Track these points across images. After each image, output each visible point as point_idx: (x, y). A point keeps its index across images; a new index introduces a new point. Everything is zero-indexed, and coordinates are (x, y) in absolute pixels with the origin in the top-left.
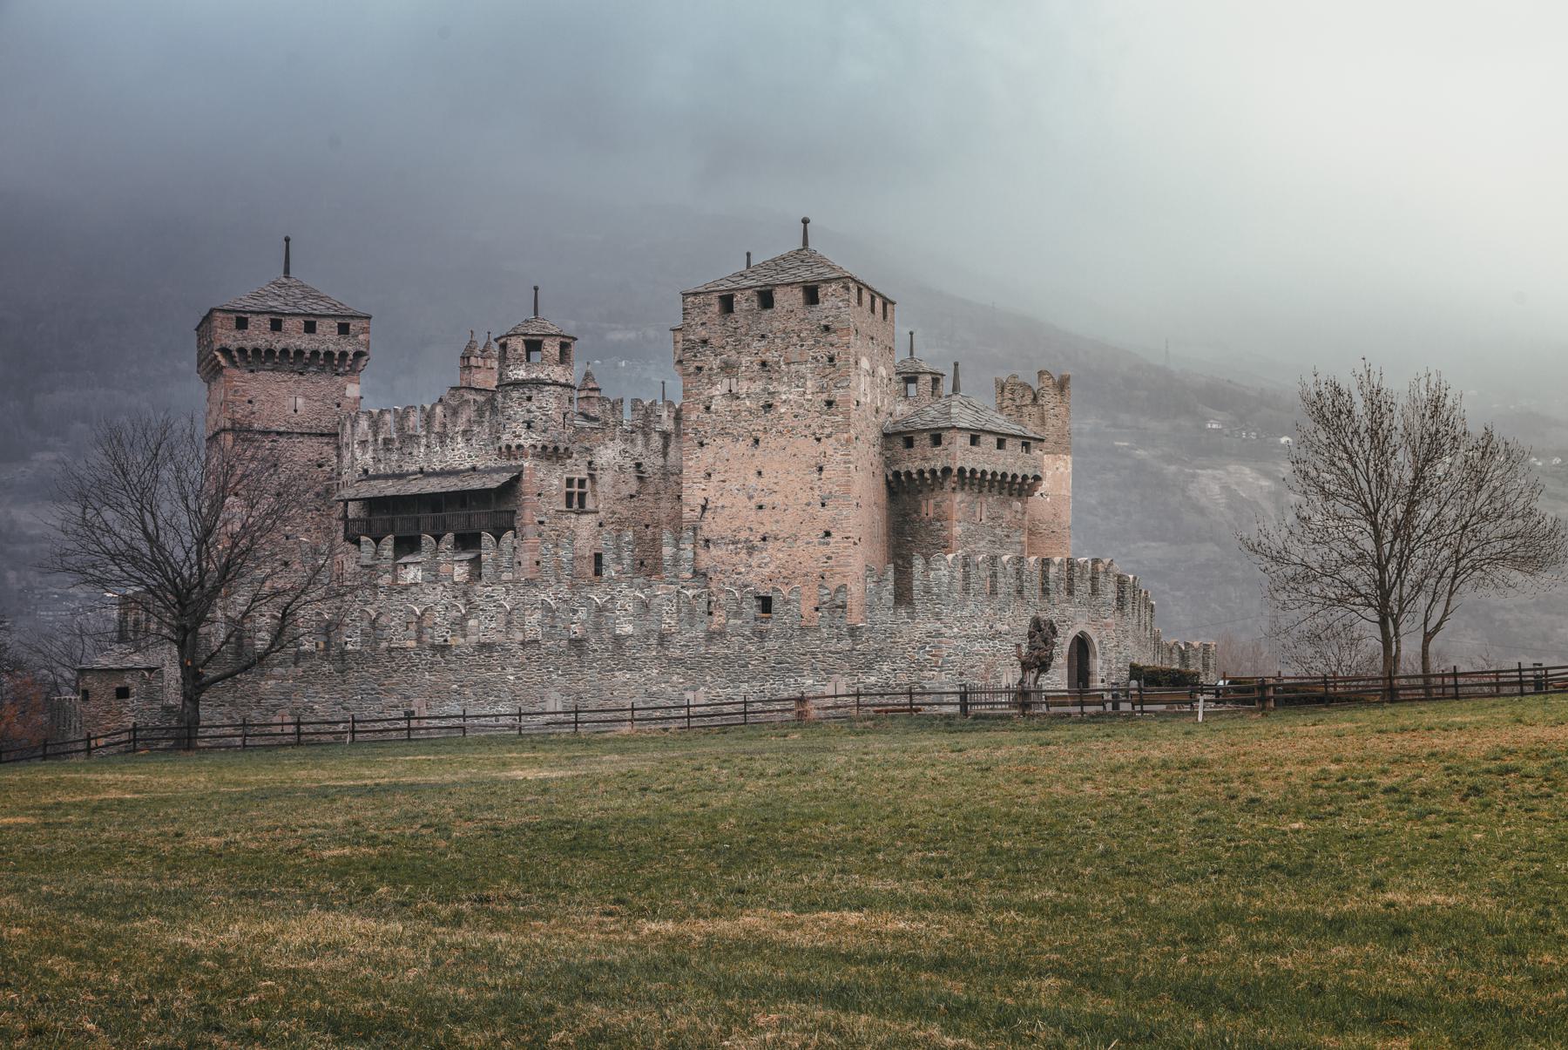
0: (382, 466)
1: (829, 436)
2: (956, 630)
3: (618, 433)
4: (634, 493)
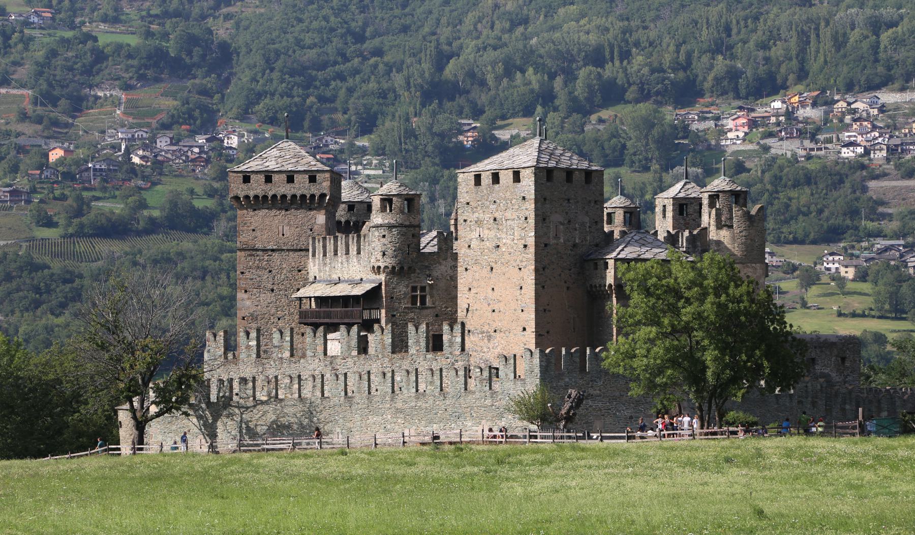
0: (322, 274)
1: (525, 268)
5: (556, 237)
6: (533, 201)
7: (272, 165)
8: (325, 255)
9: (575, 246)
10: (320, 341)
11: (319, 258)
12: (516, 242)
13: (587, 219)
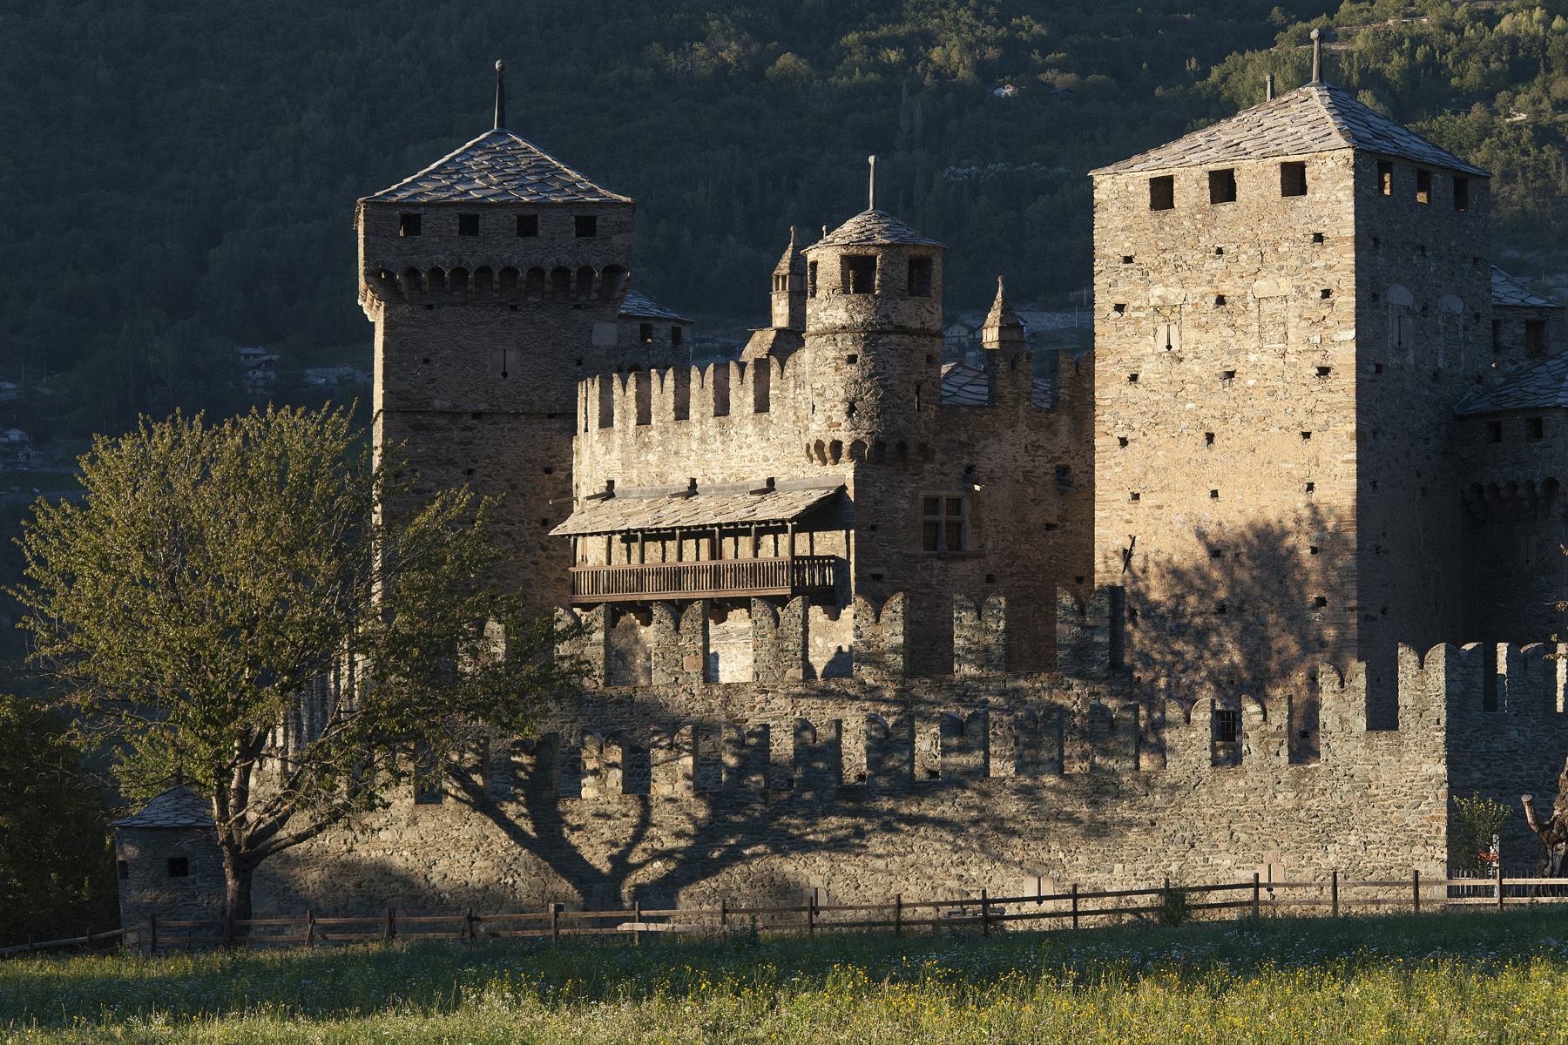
0: (634, 473)
2: (1477, 775)
3: (1022, 413)
4: (1052, 520)
5: (1400, 349)
6: (1350, 245)
7: (477, 189)
9: (1436, 376)
10: (690, 643)
11: (624, 432)
12: (1292, 359)
13: (1458, 306)
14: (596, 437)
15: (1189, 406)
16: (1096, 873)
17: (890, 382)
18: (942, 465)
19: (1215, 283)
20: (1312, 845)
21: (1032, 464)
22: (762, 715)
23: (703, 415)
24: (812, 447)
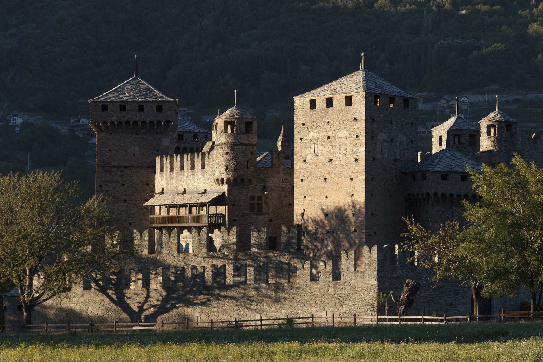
0: (169, 186)
2: (387, 284)
3: (281, 169)
5: (382, 153)
6: (364, 122)
7: (126, 97)
8: (172, 170)
9: (396, 160)
11: (166, 173)
12: (348, 156)
13: (405, 138)
14: (159, 175)
15: (320, 170)
16: (277, 313)
17: (239, 160)
18: (256, 185)
19: (327, 132)
20: (339, 305)
21: (284, 185)
22: (195, 263)
23: (187, 169)
24: (216, 180)
